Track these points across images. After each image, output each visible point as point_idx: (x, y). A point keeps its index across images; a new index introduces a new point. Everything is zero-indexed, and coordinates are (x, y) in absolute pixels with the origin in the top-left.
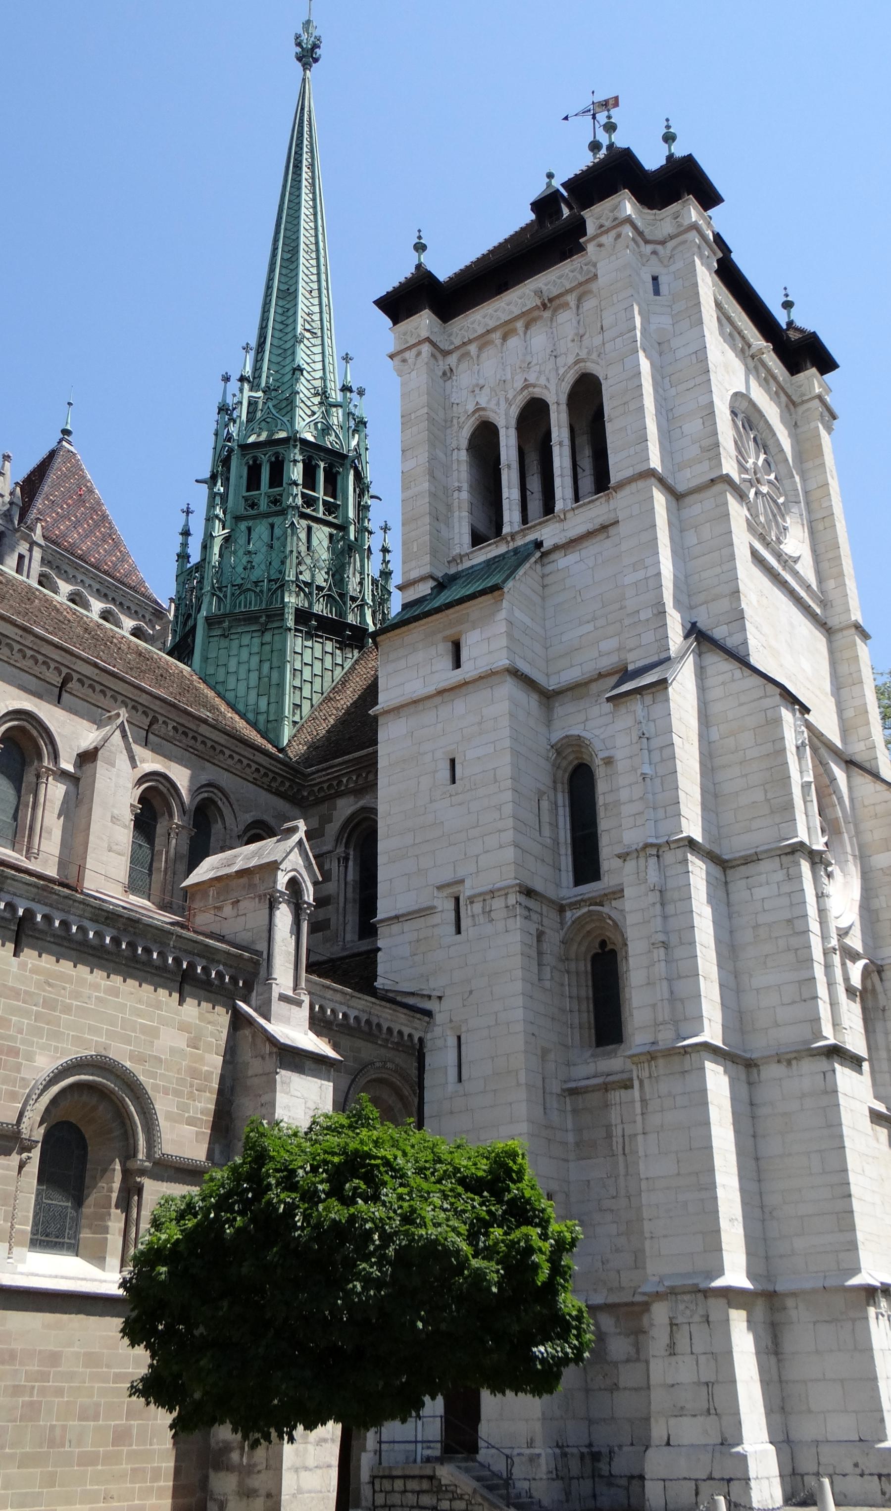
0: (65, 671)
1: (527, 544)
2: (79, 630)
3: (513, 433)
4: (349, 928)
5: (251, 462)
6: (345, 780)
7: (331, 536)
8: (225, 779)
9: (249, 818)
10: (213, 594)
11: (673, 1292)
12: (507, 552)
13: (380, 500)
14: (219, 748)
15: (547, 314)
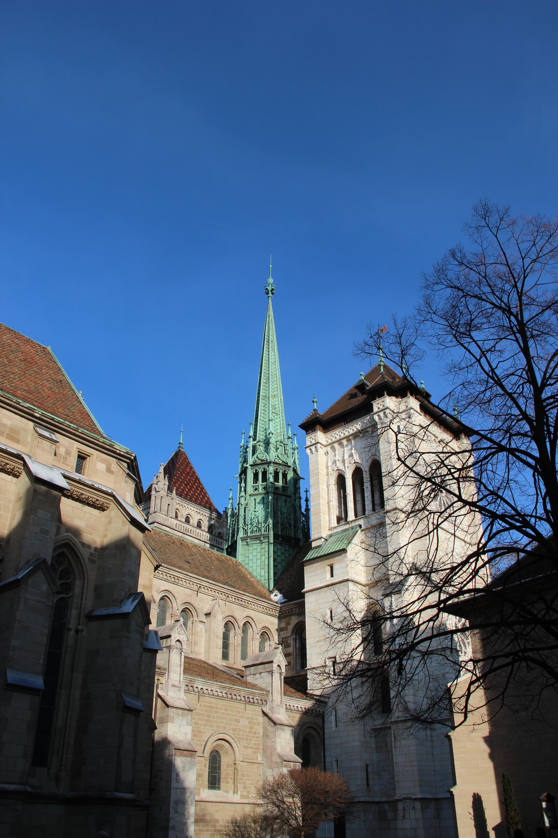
0: (199, 586)
1: (356, 525)
2: (198, 556)
3: (351, 480)
4: (298, 665)
5: (254, 472)
6: (294, 610)
7: (286, 501)
8: (252, 613)
9: (260, 626)
10: (243, 528)
11: (405, 799)
12: (349, 528)
13: (304, 479)
14: (250, 603)
15: (361, 435)
